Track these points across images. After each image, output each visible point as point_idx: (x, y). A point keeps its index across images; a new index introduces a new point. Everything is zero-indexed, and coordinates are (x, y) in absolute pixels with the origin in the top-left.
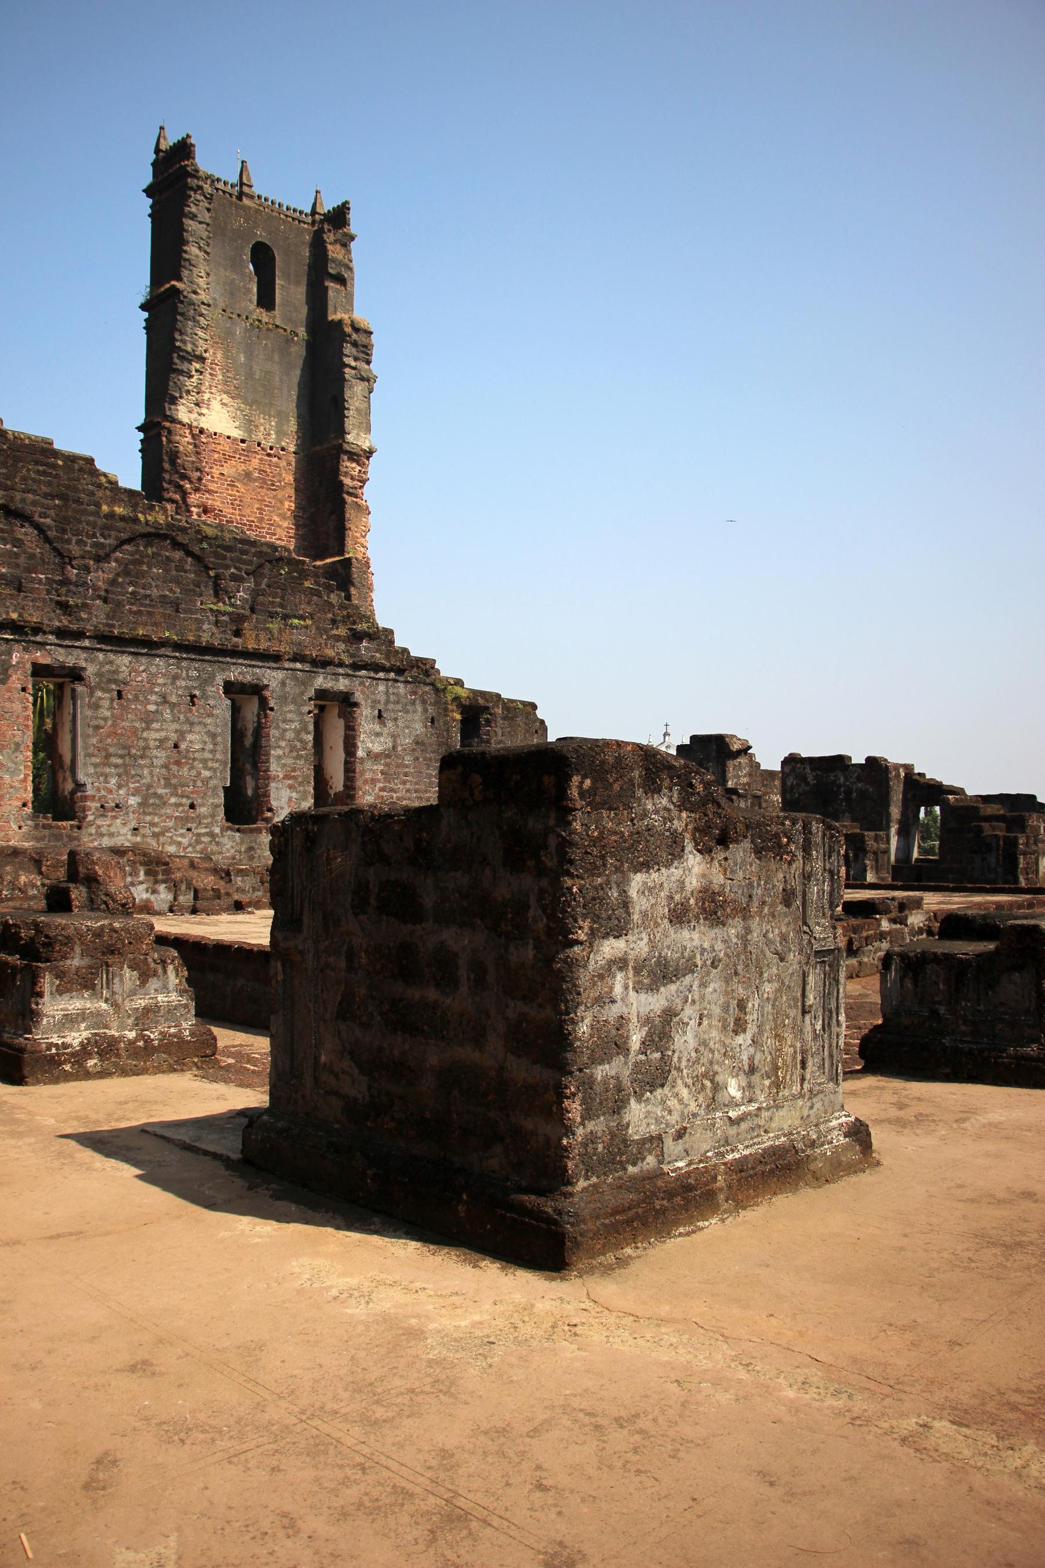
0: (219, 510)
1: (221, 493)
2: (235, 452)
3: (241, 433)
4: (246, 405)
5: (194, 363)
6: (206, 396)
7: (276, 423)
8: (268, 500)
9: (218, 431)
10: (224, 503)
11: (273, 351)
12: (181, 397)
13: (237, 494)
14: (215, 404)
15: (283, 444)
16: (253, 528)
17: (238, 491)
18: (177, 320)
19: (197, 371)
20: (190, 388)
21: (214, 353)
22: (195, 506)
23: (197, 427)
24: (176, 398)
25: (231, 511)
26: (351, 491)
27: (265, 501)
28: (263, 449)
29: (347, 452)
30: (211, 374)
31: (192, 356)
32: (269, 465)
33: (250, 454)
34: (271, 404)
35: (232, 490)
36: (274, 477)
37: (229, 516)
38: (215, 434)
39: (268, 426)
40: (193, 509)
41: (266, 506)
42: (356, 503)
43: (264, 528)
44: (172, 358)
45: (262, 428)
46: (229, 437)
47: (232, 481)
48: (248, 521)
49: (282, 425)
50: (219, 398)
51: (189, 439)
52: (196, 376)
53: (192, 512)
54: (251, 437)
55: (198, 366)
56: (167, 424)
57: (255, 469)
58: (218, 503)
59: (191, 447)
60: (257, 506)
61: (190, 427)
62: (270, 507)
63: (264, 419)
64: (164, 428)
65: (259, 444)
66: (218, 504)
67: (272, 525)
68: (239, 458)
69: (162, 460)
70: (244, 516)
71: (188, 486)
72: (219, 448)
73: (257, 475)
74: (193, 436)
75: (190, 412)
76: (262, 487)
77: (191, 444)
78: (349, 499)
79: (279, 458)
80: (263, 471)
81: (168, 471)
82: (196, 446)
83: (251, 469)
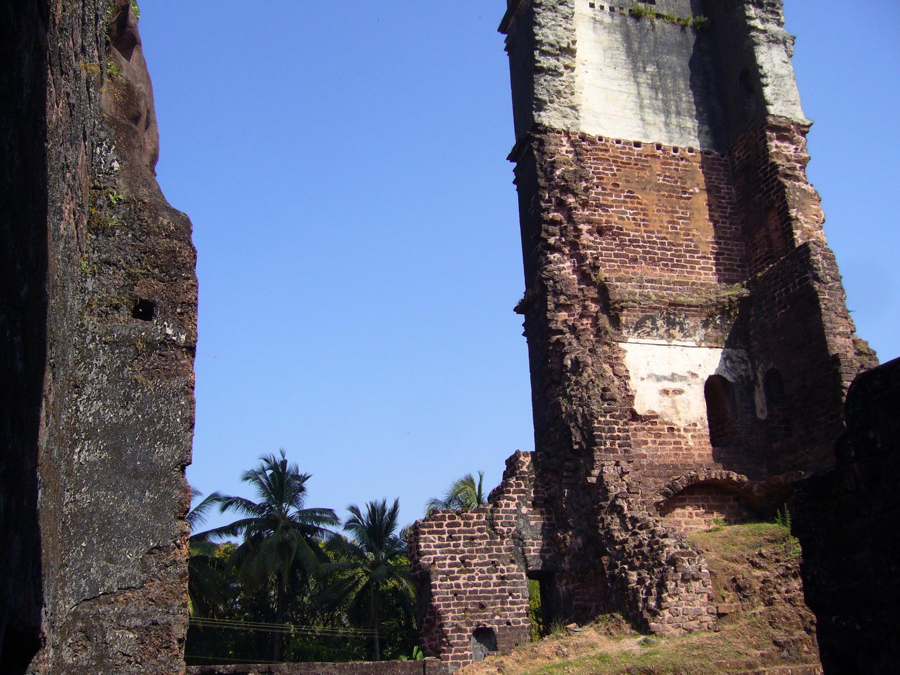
0: (617, 228)
1: (616, 207)
5: (561, 59)
8: (681, 211)
10: (622, 219)
12: (552, 102)
16: (667, 247)
17: (640, 203)
18: (535, 13)
20: (561, 88)
22: (584, 223)
24: (545, 102)
25: (634, 228)
26: (789, 172)
29: (774, 128)
35: (632, 203)
37: (632, 234)
38: (601, 139)
40: (581, 226)
43: (681, 245)
44: (534, 56)
46: (618, 142)
47: (629, 192)
48: (658, 238)
51: (566, 147)
52: (566, 73)
53: (581, 230)
56: (538, 136)
59: (571, 156)
61: (567, 134)
62: (685, 219)
64: (536, 139)
67: (691, 240)
69: (537, 176)
70: (653, 232)
71: (571, 200)
74: (573, 144)
75: (564, 117)
76: (671, 196)
77: (570, 152)
78: (788, 183)
79: (687, 160)
81: (544, 188)
82: (577, 154)
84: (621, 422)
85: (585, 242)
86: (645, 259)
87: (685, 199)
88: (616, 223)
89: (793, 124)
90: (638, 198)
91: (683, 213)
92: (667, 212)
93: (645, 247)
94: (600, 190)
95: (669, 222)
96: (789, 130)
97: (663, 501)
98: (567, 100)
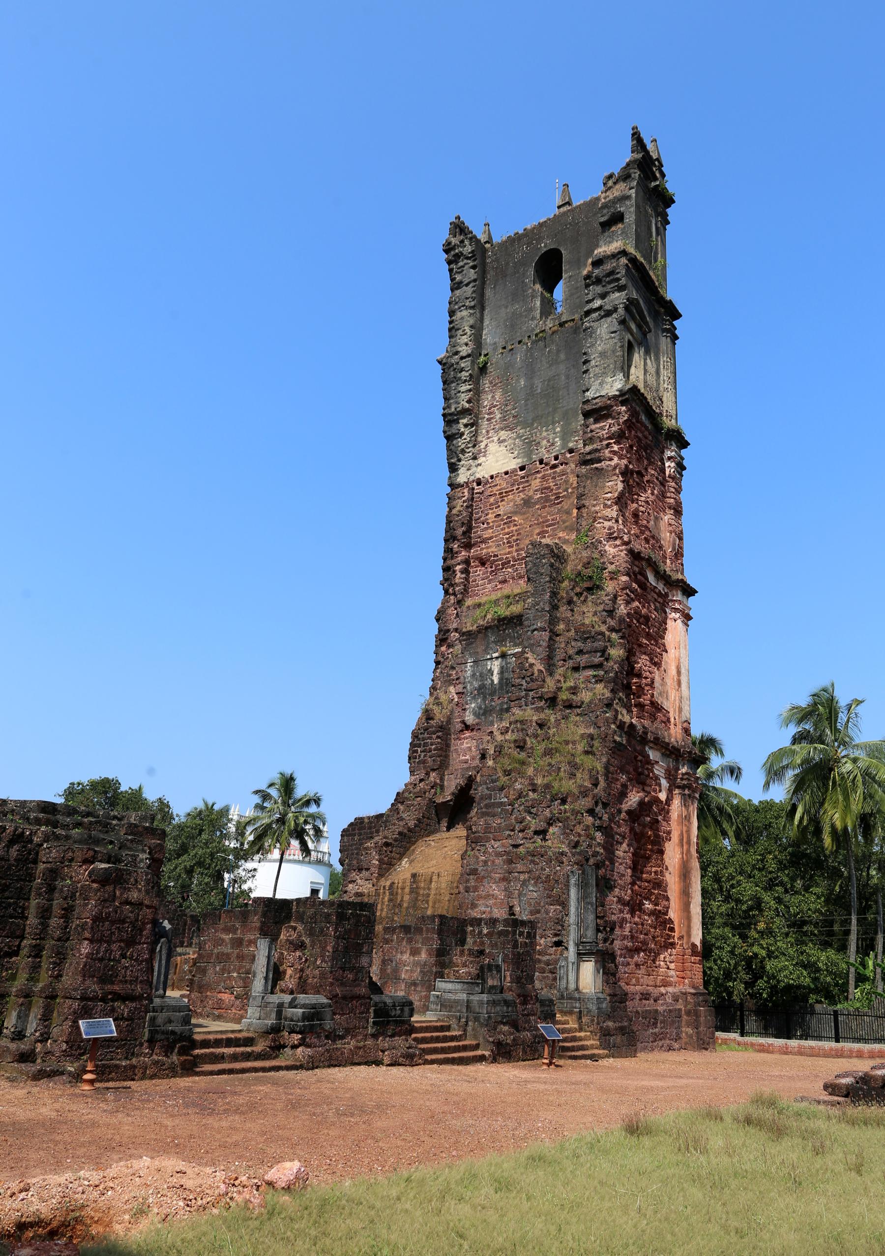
1: (496, 536)
2: (513, 485)
3: (520, 460)
4: (525, 428)
5: (460, 421)
6: (483, 445)
7: (562, 426)
9: (494, 473)
11: (558, 351)
12: (460, 460)
13: (515, 528)
14: (493, 447)
15: (571, 445)
17: (516, 525)
19: (466, 426)
21: (493, 397)
22: (459, 564)
23: (473, 481)
25: (508, 550)
27: (548, 521)
28: (546, 464)
30: (489, 420)
31: (456, 415)
32: (554, 478)
33: (530, 478)
34: (555, 410)
35: (509, 527)
36: (559, 488)
38: (492, 477)
39: (551, 436)
41: (548, 526)
42: (596, 468)
45: (544, 442)
46: (506, 473)
49: (570, 424)
50: (496, 439)
54: (531, 459)
55: (465, 421)
57: (536, 491)
58: (493, 549)
60: (537, 531)
63: (546, 431)
65: (541, 462)
66: (493, 550)
68: (518, 489)
72: (495, 489)
73: (539, 496)
76: (544, 507)
80: (545, 488)
83: (531, 493)
84: (434, 736)
85: (457, 581)
86: (513, 578)
87: (558, 504)
88: (492, 552)
89: (609, 399)
90: (515, 521)
91: (553, 520)
92: (538, 524)
93: (515, 565)
94: (485, 525)
95: (538, 534)
96: (608, 407)
97: (451, 800)
98: (471, 454)
